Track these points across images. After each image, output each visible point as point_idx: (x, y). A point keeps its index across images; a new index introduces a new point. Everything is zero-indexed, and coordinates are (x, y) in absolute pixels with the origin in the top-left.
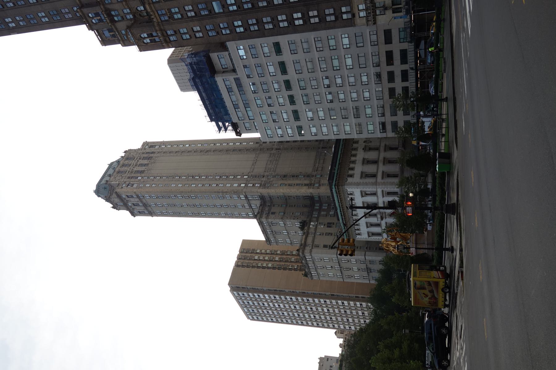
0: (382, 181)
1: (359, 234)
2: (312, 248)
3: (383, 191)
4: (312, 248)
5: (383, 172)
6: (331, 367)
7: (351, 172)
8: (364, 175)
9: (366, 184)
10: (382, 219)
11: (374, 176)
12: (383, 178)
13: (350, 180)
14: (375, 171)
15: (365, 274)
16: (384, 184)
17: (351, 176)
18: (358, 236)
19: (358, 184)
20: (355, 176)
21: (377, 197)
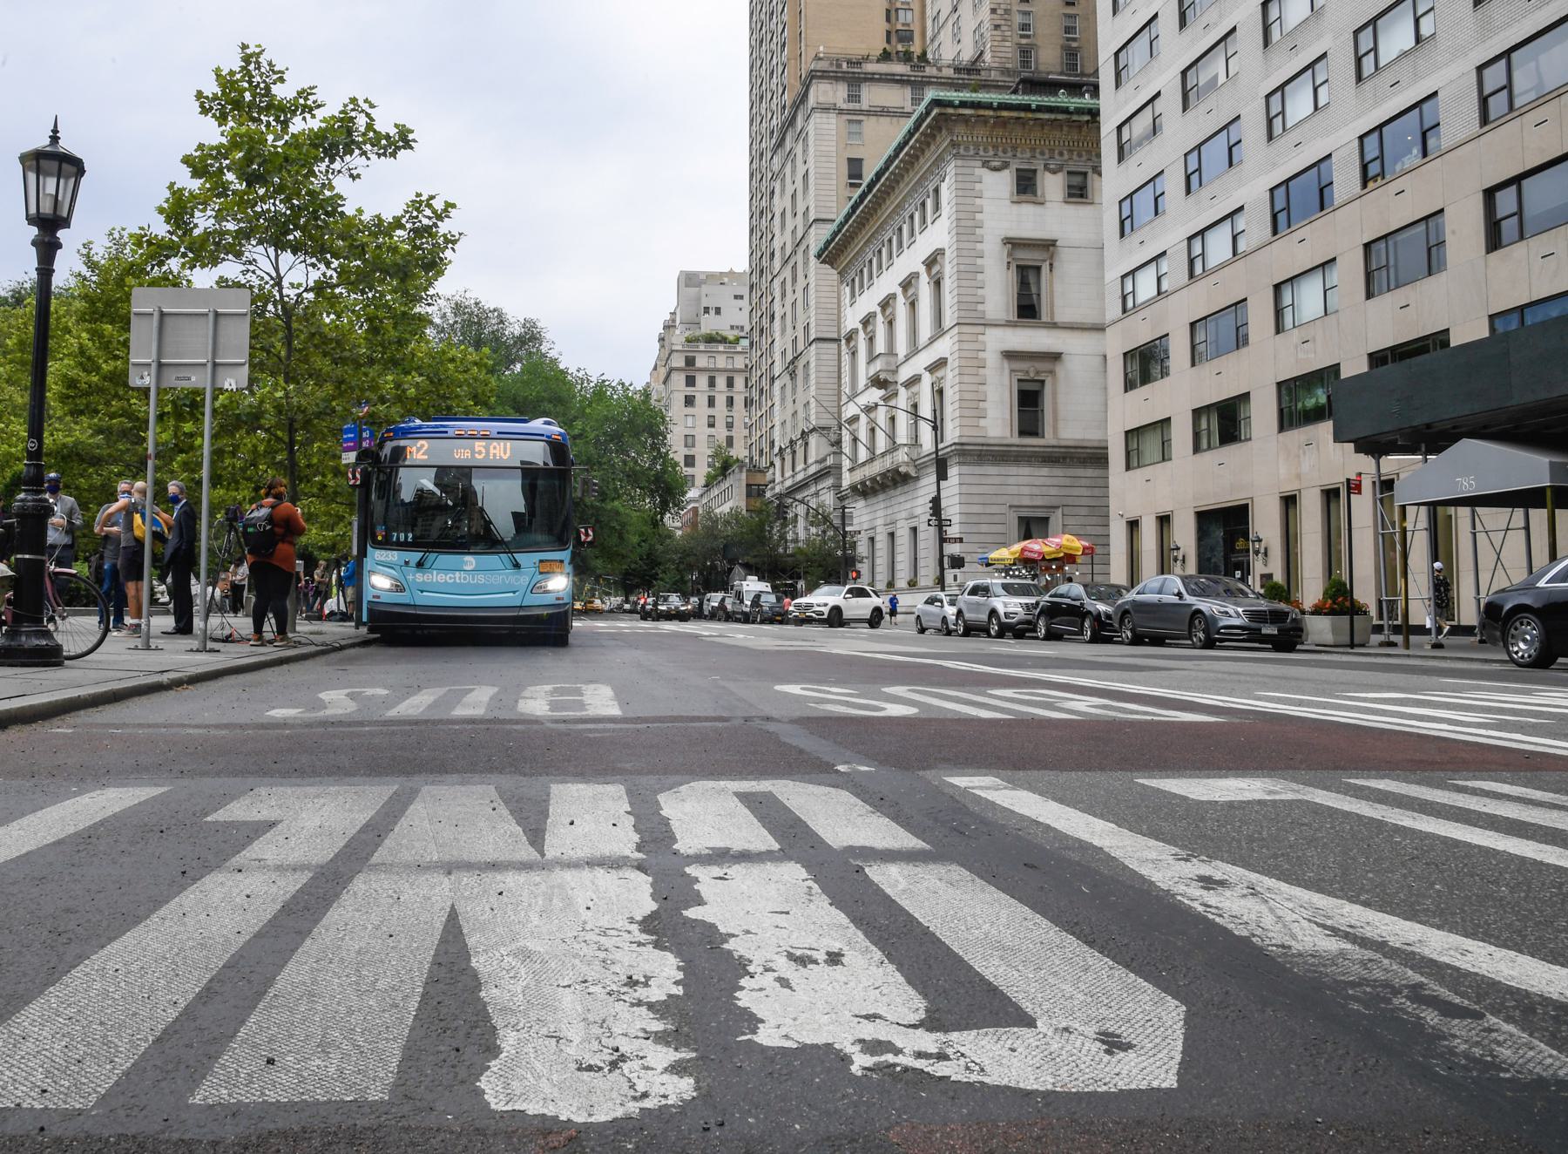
0: (992, 358)
1: (853, 295)
2: (841, 112)
3: (941, 363)
4: (841, 112)
5: (1056, 357)
6: (718, 311)
7: (1052, 185)
8: (1028, 257)
9: (970, 272)
10: (877, 382)
11: (1028, 310)
12: (1010, 355)
13: (999, 184)
14: (1060, 318)
15: (789, 357)
16: (973, 364)
17: (1026, 185)
18: (848, 290)
19: (967, 229)
20: (1028, 210)
21: (932, 340)
